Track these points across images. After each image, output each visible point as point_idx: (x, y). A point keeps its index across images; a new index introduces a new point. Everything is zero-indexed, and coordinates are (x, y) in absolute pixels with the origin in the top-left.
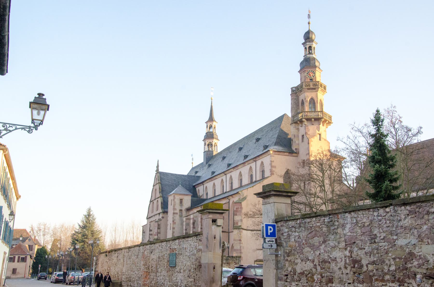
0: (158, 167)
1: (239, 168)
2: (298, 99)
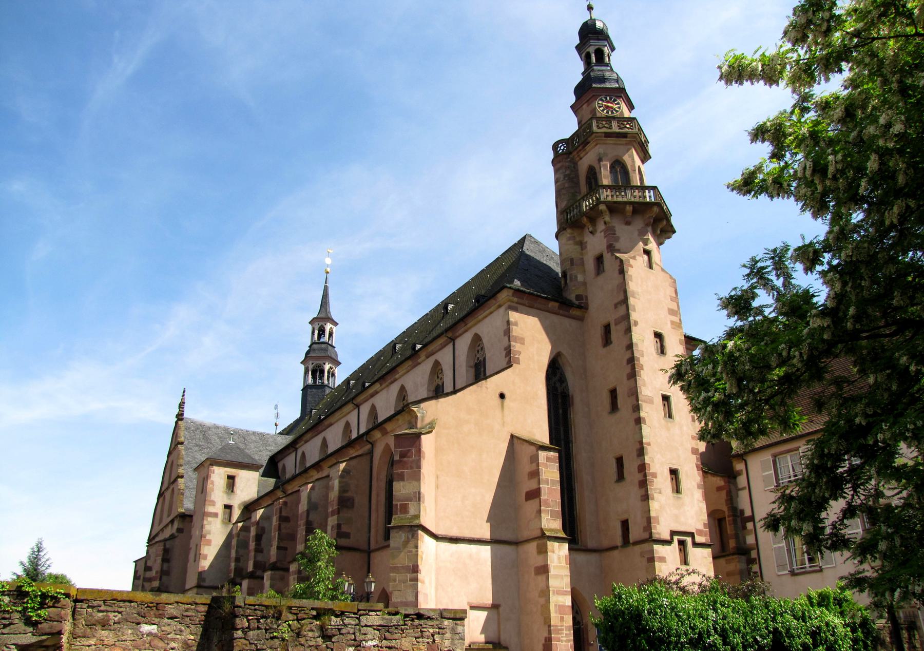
0: (181, 405)
1: (397, 376)
2: (574, 167)
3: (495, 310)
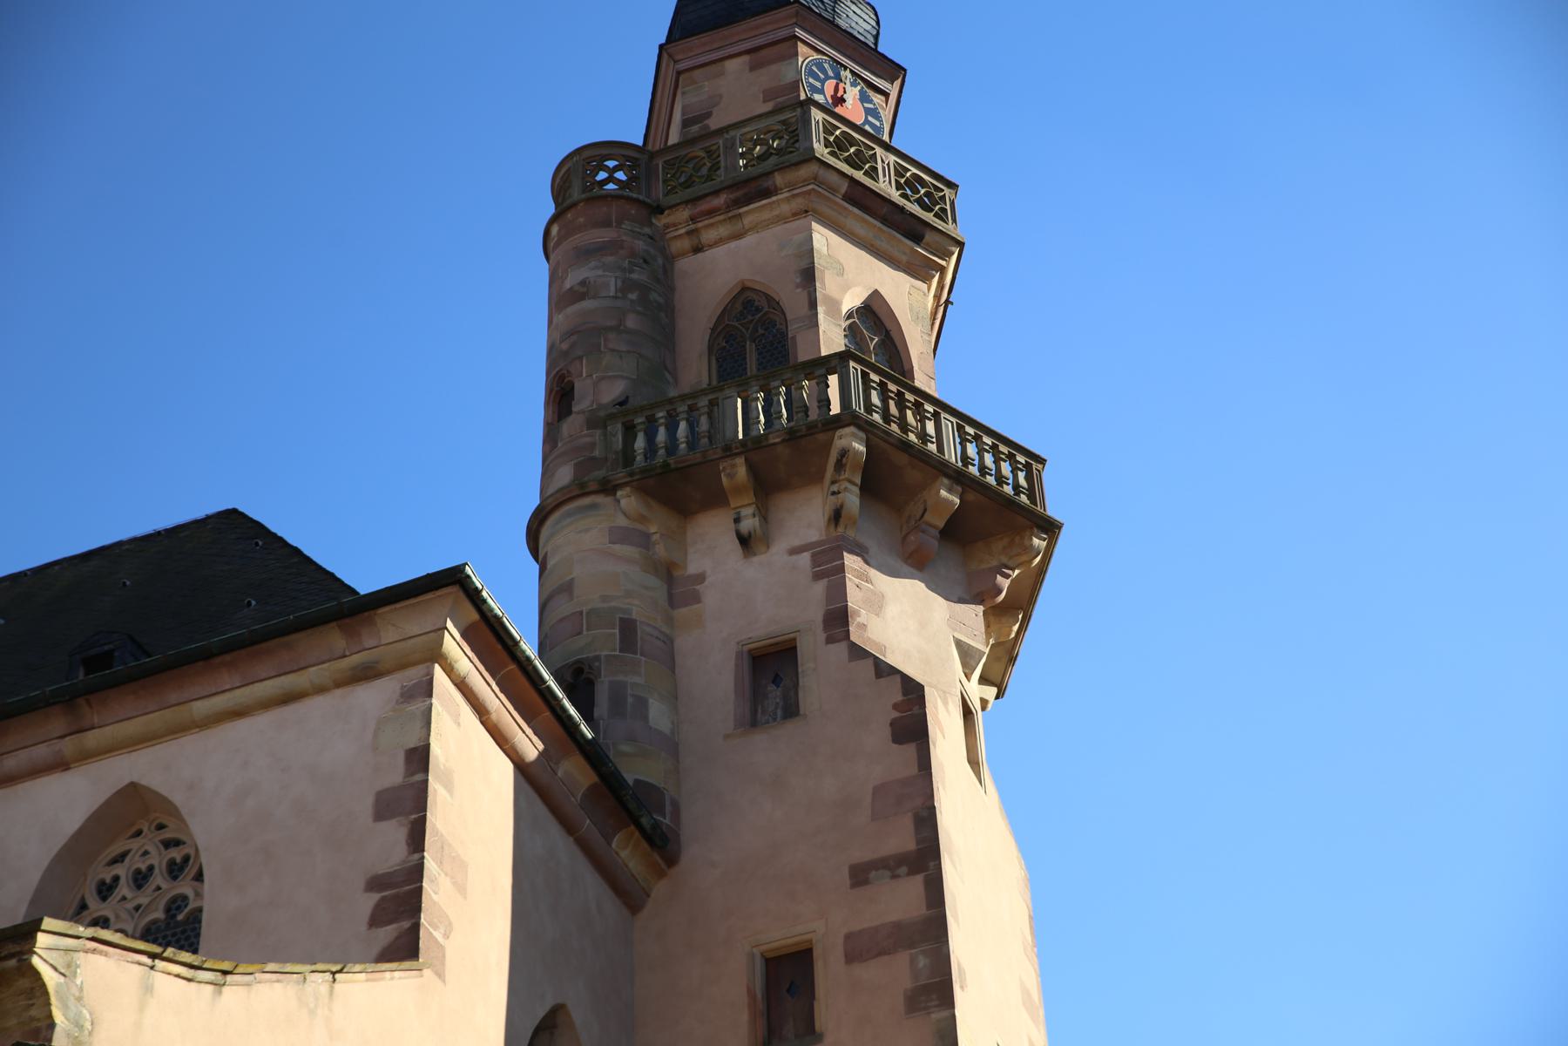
3: (321, 690)
